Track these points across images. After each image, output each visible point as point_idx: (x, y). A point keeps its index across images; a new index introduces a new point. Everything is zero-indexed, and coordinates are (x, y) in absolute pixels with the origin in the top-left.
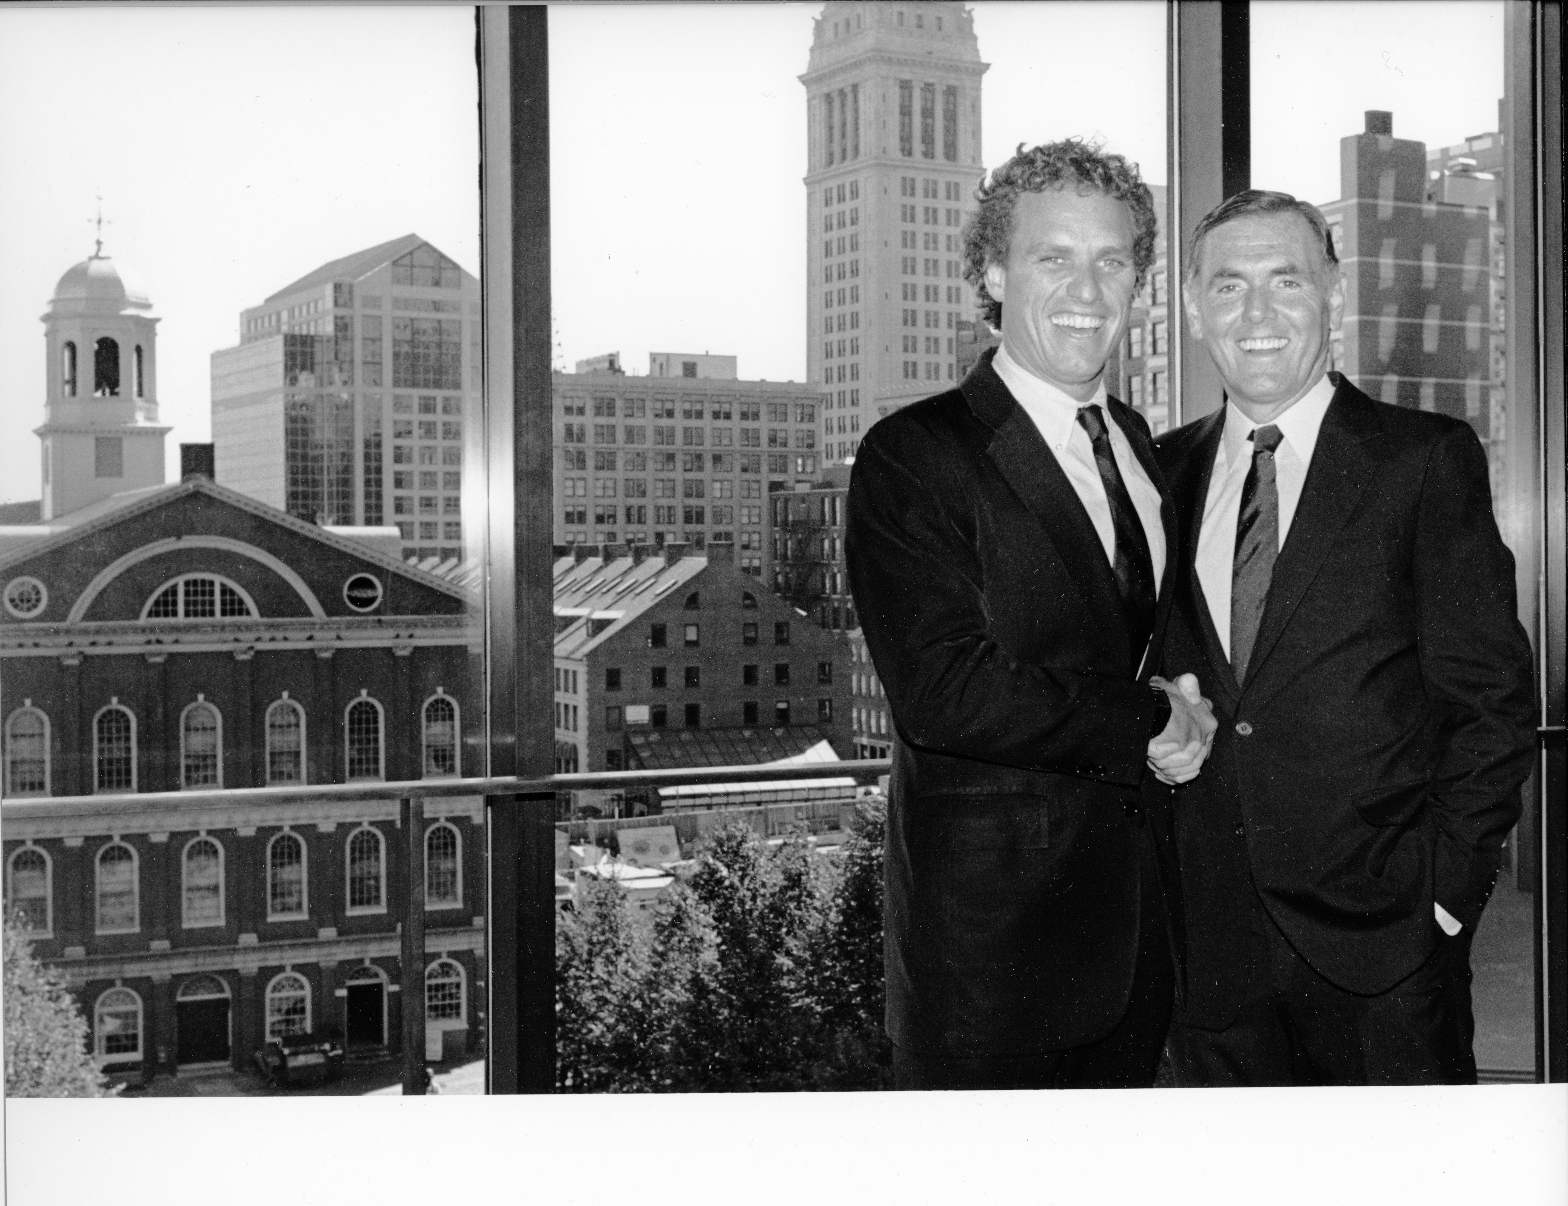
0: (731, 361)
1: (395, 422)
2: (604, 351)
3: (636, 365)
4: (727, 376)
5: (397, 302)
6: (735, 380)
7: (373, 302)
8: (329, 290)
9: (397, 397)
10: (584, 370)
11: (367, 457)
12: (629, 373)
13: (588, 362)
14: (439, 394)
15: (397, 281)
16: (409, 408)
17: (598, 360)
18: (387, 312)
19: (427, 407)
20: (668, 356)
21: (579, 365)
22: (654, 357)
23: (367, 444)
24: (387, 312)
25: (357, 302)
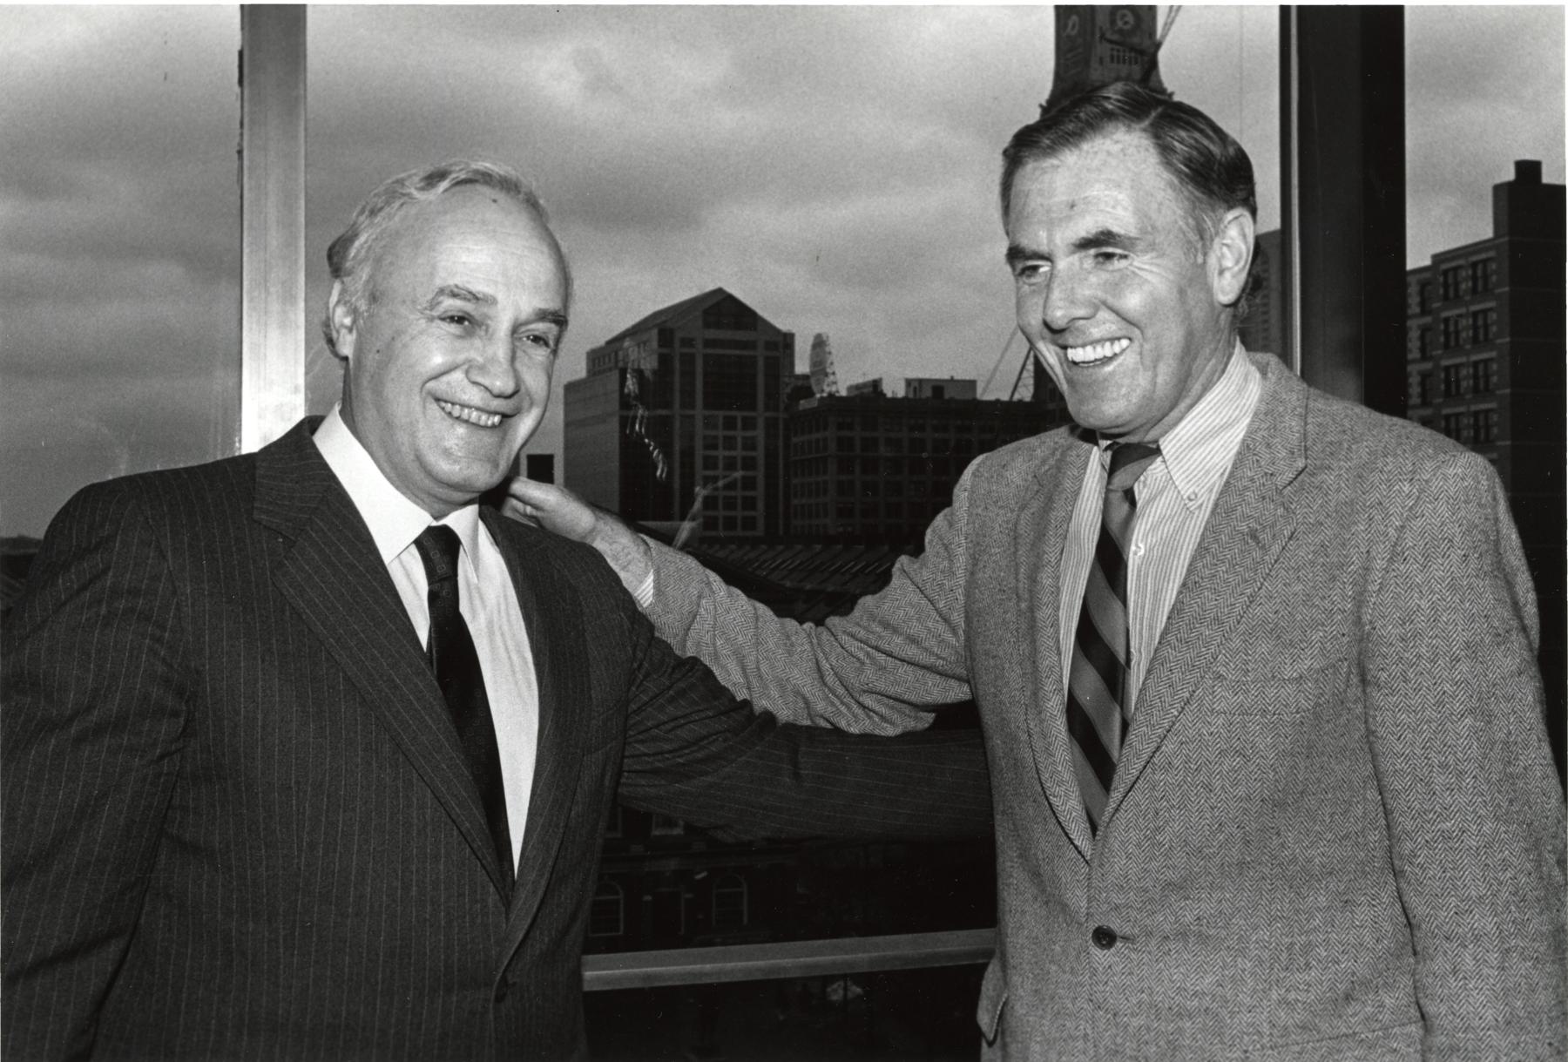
0: (972, 384)
1: (705, 437)
2: (870, 378)
3: (894, 388)
4: (968, 397)
5: (708, 343)
6: (975, 399)
7: (688, 342)
8: (655, 332)
9: (705, 418)
10: (855, 393)
11: (683, 465)
12: (889, 395)
13: (858, 387)
14: (739, 414)
15: (707, 325)
16: (715, 427)
17: (865, 385)
18: (699, 350)
19: (730, 423)
20: (921, 381)
21: (850, 388)
22: (909, 382)
23: (683, 453)
24: (699, 350)
25: (677, 344)
